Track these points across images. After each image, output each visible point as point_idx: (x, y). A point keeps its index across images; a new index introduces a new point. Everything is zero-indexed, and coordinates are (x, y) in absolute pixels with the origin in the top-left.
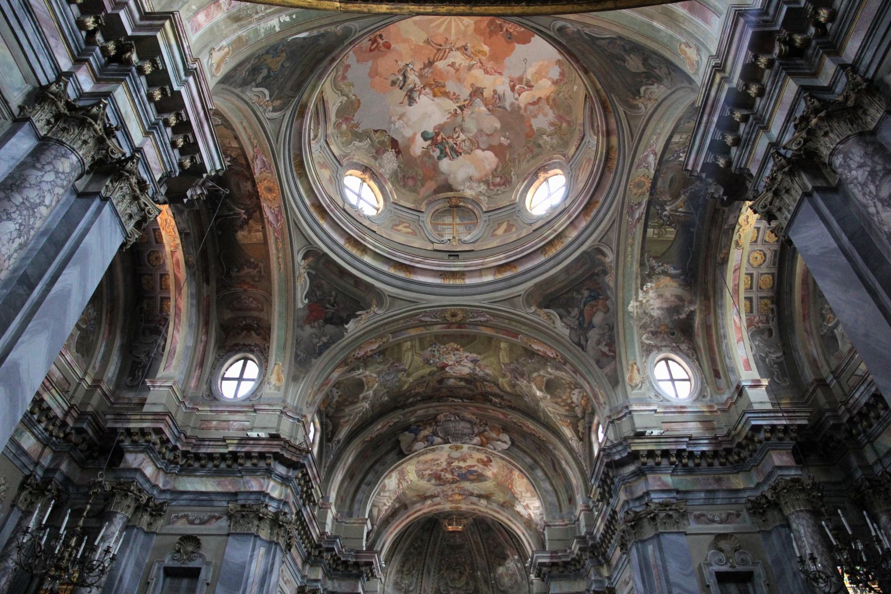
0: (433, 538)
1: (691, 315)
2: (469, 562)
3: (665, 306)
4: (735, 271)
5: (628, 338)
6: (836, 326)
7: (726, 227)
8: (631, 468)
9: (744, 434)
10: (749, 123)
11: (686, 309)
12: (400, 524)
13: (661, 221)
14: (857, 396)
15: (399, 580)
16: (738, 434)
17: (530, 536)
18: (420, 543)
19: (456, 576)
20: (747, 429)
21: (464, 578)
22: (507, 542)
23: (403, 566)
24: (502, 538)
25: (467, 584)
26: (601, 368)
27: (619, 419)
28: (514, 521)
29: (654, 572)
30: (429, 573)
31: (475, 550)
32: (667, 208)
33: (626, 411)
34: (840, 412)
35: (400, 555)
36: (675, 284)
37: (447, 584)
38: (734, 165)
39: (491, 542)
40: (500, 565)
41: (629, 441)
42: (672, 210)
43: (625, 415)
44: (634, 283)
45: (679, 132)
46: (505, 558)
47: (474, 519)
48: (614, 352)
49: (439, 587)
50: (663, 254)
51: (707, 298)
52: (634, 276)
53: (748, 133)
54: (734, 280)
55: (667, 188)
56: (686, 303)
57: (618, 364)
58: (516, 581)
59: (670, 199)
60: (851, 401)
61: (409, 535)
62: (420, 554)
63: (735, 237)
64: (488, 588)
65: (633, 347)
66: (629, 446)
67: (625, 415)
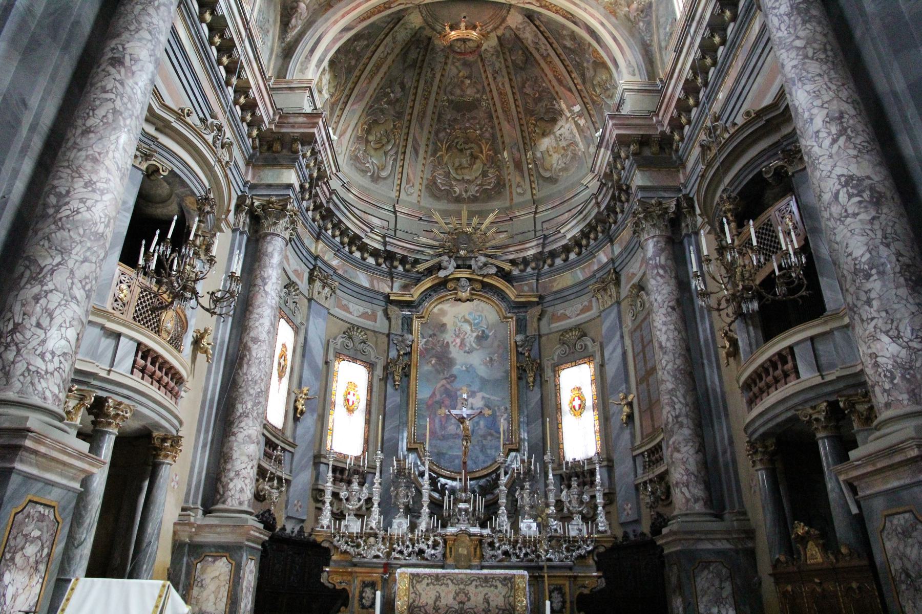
0: (422, 82)
2: (487, 135)
12: (355, 8)
15: (360, 154)
17: (615, 27)
18: (398, 89)
19: (465, 161)
21: (478, 166)
22: (560, 82)
23: (368, 131)
24: (550, 75)
25: (484, 174)
28: (582, 5)
30: (416, 152)
31: (500, 111)
35: (363, 103)
37: (447, 175)
39: (528, 90)
40: (544, 135)
46: (553, 117)
47: (499, 38)
49: (434, 178)
58: (575, 156)
61: (378, 67)
62: (399, 115)
64: (523, 177)
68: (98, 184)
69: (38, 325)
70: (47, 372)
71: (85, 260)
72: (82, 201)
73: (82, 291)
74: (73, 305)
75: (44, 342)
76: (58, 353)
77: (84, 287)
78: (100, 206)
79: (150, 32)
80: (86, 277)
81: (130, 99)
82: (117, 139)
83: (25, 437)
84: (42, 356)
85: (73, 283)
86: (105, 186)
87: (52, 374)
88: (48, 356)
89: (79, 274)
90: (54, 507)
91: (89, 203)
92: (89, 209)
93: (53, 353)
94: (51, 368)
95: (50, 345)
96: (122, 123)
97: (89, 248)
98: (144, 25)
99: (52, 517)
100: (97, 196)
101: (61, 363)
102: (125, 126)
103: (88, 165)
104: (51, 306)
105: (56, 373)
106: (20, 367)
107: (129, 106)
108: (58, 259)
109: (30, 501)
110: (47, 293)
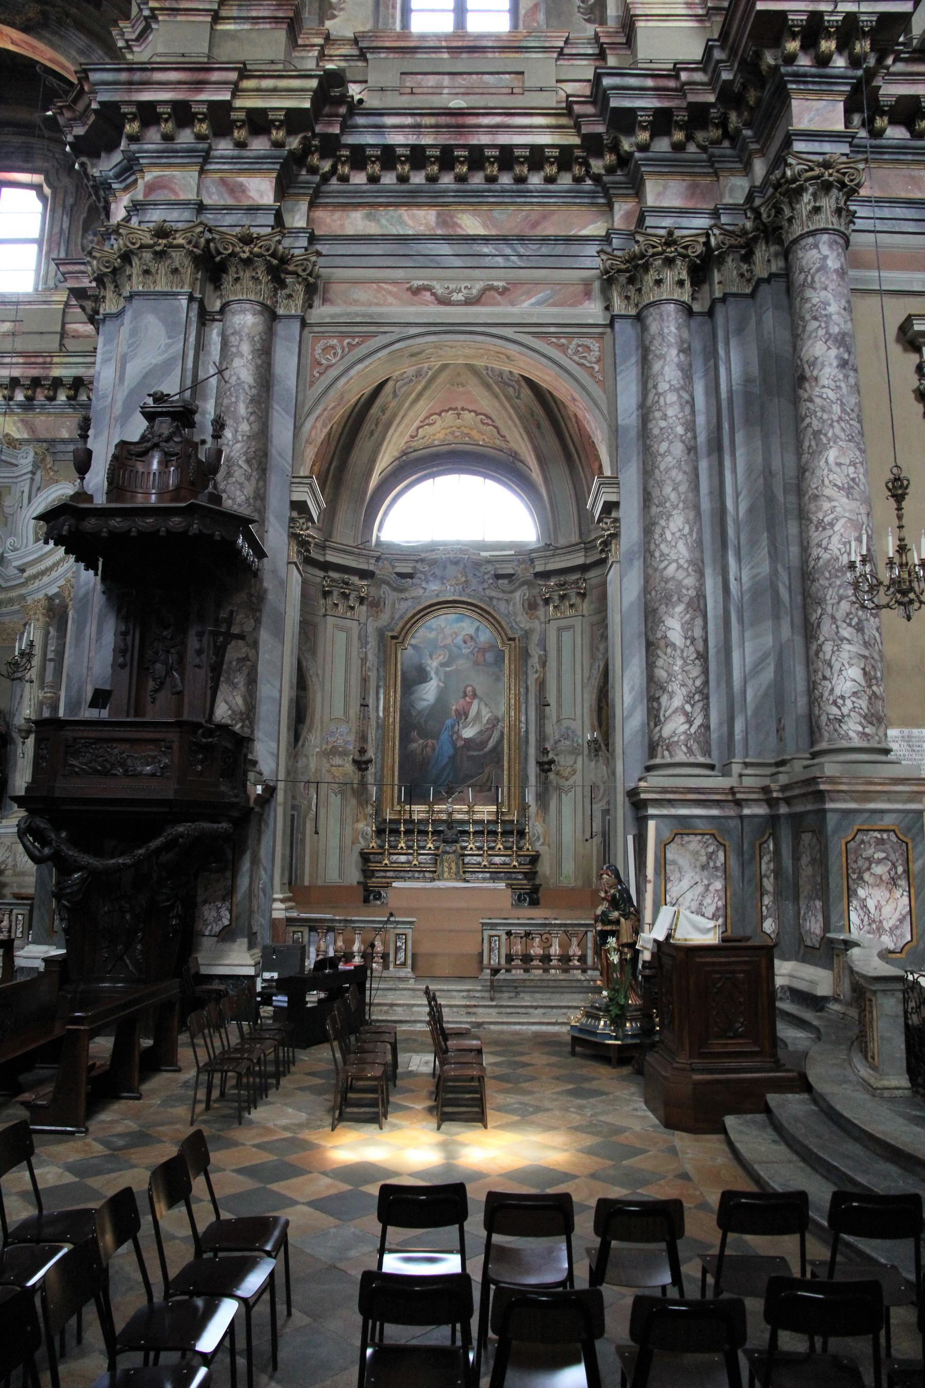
68: (826, 520)
69: (825, 678)
70: (843, 716)
71: (841, 598)
72: (819, 545)
73: (850, 629)
74: (846, 646)
75: (832, 690)
76: (847, 695)
77: (850, 625)
78: (835, 539)
79: (815, 318)
80: (848, 614)
81: (823, 410)
82: (827, 462)
83: (818, 783)
84: (835, 703)
85: (837, 627)
86: (832, 516)
87: (849, 716)
88: (840, 701)
89: (839, 615)
90: (894, 831)
91: (824, 543)
92: (826, 549)
93: (843, 697)
94: (845, 710)
95: (837, 692)
96: (825, 441)
97: (840, 586)
98: (808, 317)
99: (894, 839)
100: (829, 532)
101: (853, 702)
102: (829, 440)
103: (812, 507)
104: (828, 657)
105: (852, 714)
106: (824, 718)
107: (825, 416)
108: (819, 611)
109: (859, 830)
110: (820, 646)
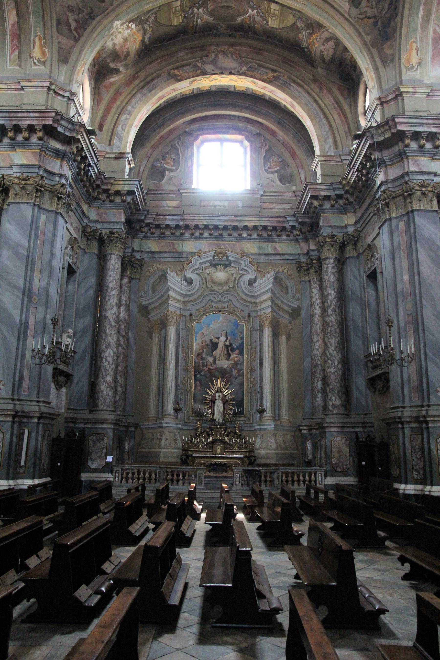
1: (116, 71)
3: (117, 48)
4: (172, 89)
5: (96, 40)
6: (170, 170)
7: (199, 65)
8: (58, 146)
9: (119, 188)
10: (434, 150)
11: (119, 65)
13: (187, 9)
14: (168, 217)
16: (112, 184)
20: (126, 188)
26: (58, 32)
27: (56, 93)
29: (40, 236)
32: (200, 10)
33: (67, 94)
34: (150, 216)
36: (137, 46)
38: (407, 149)
41: (82, 130)
42: (198, 14)
43: (64, 97)
44: (133, 14)
45: (282, 9)
48: (80, 36)
50: (160, 24)
51: (134, 77)
52: (141, 10)
53: (428, 151)
54: (166, 93)
55: (220, 5)
56: (124, 62)
57: (76, 50)
59: (209, 9)
60: (161, 217)
63: (198, 78)
65: (92, 51)
66: (78, 132)
67: (64, 97)
